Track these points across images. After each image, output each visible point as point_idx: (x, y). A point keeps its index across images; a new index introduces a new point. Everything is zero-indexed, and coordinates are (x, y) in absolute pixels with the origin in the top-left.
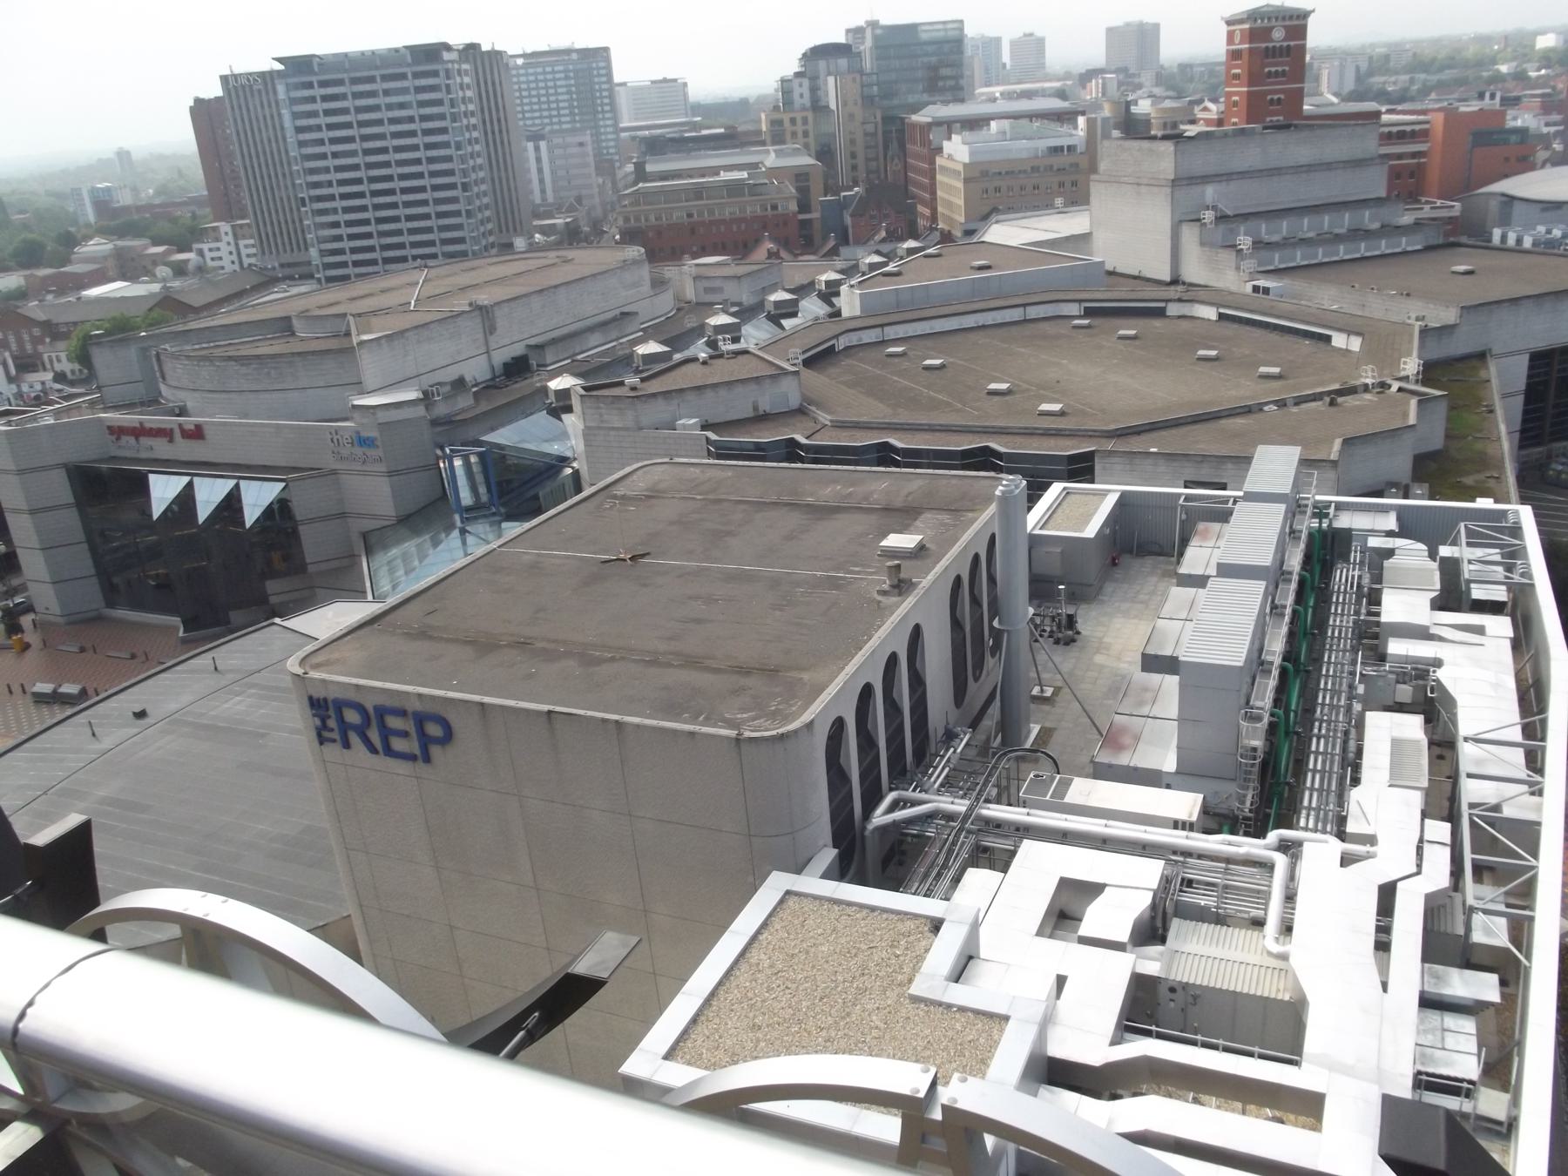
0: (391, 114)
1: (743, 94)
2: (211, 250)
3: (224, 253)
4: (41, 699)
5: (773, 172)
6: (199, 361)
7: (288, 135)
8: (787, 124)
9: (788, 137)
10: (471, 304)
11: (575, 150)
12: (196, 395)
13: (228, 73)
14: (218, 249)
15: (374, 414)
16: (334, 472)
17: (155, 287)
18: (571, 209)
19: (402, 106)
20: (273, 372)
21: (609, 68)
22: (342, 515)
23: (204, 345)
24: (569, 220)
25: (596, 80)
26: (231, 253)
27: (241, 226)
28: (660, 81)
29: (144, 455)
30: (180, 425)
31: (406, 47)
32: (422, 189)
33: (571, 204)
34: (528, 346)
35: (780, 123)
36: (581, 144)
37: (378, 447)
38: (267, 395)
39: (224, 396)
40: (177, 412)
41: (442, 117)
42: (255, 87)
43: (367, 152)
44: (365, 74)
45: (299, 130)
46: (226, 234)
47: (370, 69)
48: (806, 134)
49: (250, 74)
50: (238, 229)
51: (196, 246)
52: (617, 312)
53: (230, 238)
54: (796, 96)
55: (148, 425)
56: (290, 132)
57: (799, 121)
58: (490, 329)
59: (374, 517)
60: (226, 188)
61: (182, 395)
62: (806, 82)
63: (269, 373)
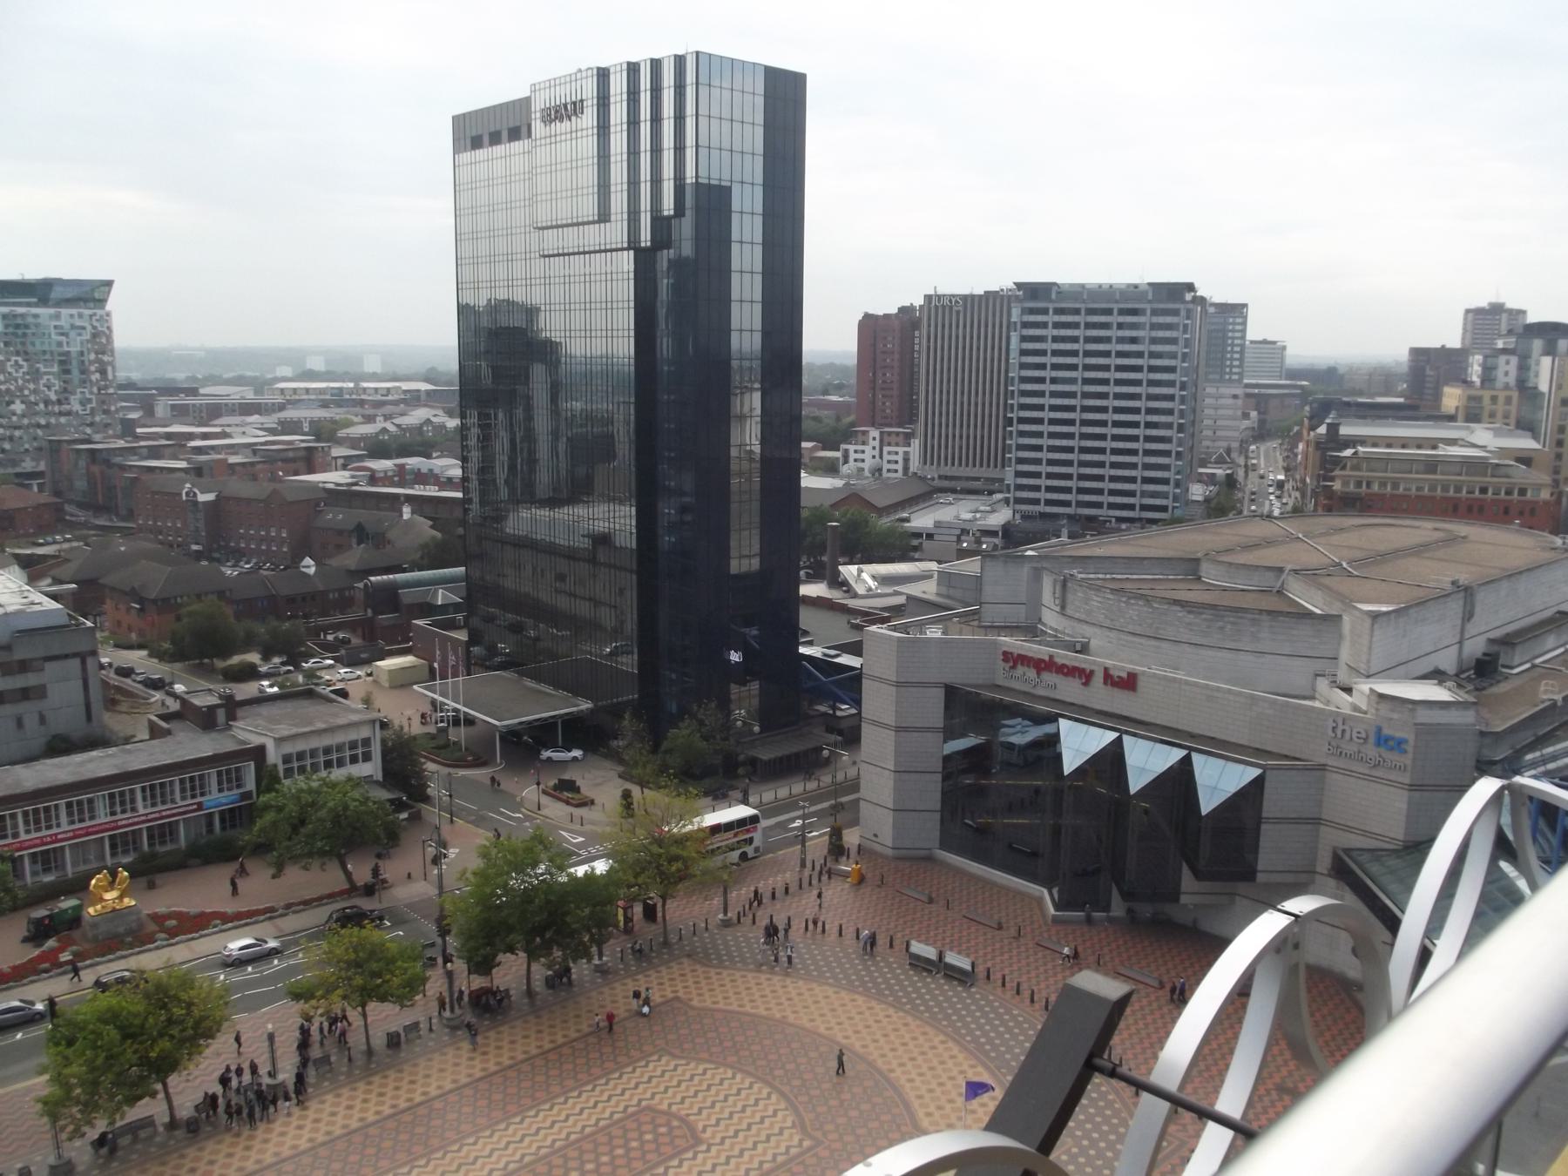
0: (1120, 347)
1: (1332, 363)
2: (856, 452)
3: (867, 456)
4: (919, 963)
5: (1503, 452)
6: (1130, 598)
7: (1012, 356)
8: (1486, 401)
9: (1486, 414)
10: (1453, 583)
11: (1231, 401)
12: (1113, 634)
13: (932, 293)
14: (863, 452)
15: (1412, 710)
16: (1322, 768)
17: (838, 483)
18: (1220, 461)
19: (1134, 340)
20: (1229, 626)
21: (1244, 323)
22: (1316, 821)
23: (1100, 576)
24: (1229, 472)
25: (1230, 334)
26: (874, 457)
27: (889, 434)
28: (1260, 342)
29: (1041, 692)
30: (1106, 670)
31: (1150, 284)
32: (1136, 425)
33: (1221, 455)
34: (1492, 641)
35: (1479, 399)
36: (1235, 397)
37: (1405, 752)
38: (1210, 653)
39: (1153, 642)
40: (1078, 647)
41: (1173, 356)
42: (955, 308)
43: (1086, 381)
44: (1104, 306)
45: (1024, 353)
46: (874, 439)
47: (1108, 302)
48: (1506, 416)
49: (954, 296)
50: (885, 437)
51: (843, 446)
52: (1555, 610)
53: (876, 444)
54: (1500, 373)
55: (1059, 661)
56: (1014, 354)
57: (1501, 400)
58: (1468, 615)
59: (1366, 833)
60: (874, 395)
61: (1088, 631)
62: (1514, 360)
63: (1222, 628)
